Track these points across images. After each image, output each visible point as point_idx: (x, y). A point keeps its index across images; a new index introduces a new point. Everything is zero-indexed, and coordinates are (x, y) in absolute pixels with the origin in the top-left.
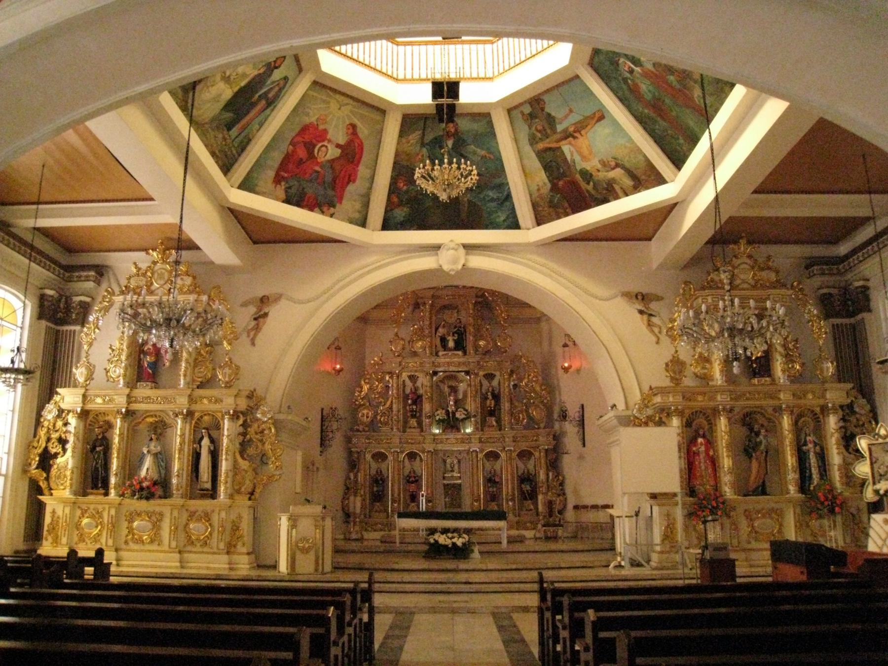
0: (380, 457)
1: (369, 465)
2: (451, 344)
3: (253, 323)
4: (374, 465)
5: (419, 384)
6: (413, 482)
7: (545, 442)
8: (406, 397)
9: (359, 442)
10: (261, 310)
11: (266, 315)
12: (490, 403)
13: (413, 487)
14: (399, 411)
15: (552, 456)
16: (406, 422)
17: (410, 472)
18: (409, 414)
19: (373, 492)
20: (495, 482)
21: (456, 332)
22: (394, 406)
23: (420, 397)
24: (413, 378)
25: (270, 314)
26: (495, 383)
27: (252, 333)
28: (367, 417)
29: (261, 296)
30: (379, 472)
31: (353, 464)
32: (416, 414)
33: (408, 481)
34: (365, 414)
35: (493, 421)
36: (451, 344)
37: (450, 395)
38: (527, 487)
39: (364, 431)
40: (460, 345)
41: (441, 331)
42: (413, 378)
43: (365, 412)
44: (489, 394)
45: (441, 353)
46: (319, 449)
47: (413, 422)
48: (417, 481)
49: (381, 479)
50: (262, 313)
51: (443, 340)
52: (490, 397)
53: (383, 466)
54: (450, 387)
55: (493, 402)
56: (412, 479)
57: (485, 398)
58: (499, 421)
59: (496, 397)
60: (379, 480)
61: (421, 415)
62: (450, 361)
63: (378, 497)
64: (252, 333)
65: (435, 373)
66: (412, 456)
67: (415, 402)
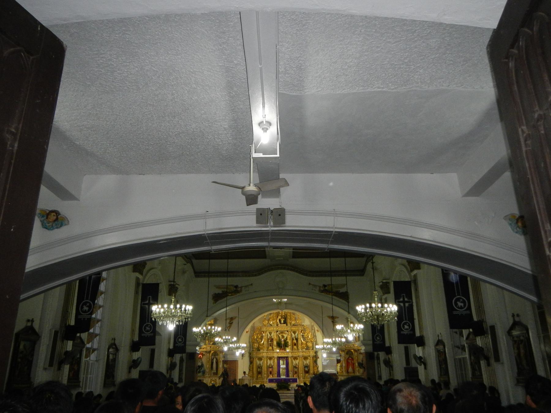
0: (260, 359)
1: (257, 362)
2: (282, 322)
3: (229, 325)
4: (258, 362)
5: (272, 335)
6: (270, 368)
7: (312, 354)
8: (268, 339)
9: (254, 354)
10: (231, 321)
11: (232, 323)
12: (295, 341)
13: (271, 369)
14: (266, 344)
15: (315, 359)
16: (268, 348)
17: (270, 364)
18: (269, 345)
19: (258, 371)
20: (297, 368)
21: (284, 318)
22: (265, 343)
23: (273, 339)
24: (270, 333)
25: (234, 322)
26: (296, 334)
27: (229, 328)
28: (256, 346)
29: (231, 317)
30: (260, 364)
31: (251, 362)
32: (271, 345)
33: (269, 367)
34: (256, 345)
35: (295, 347)
36: (282, 322)
37: (282, 338)
38: (307, 369)
39: (255, 351)
40: (285, 322)
41: (279, 317)
42: (270, 333)
43: (256, 344)
44: (294, 338)
45: (279, 325)
46: (241, 357)
47: (270, 348)
48: (272, 367)
49: (261, 367)
50: (231, 322)
51: (280, 320)
52: (295, 339)
53: (261, 362)
54: (282, 336)
55: (296, 341)
56: (270, 367)
57: (293, 340)
58: (297, 347)
59: (297, 339)
60: (260, 367)
61: (273, 345)
62: (283, 327)
63: (260, 373)
64: (229, 328)
65: (277, 331)
66: (270, 358)
67: (271, 341)
